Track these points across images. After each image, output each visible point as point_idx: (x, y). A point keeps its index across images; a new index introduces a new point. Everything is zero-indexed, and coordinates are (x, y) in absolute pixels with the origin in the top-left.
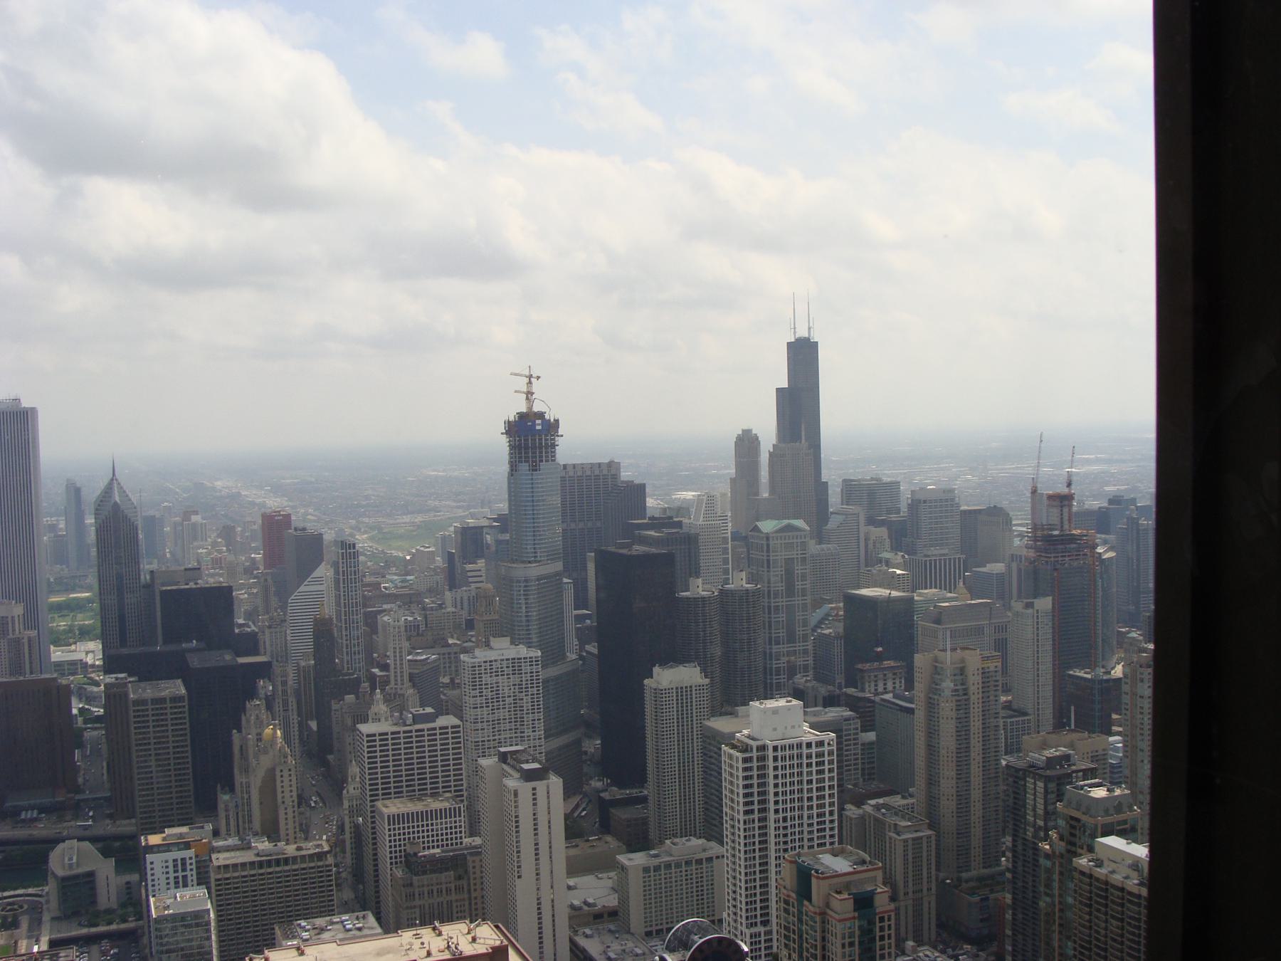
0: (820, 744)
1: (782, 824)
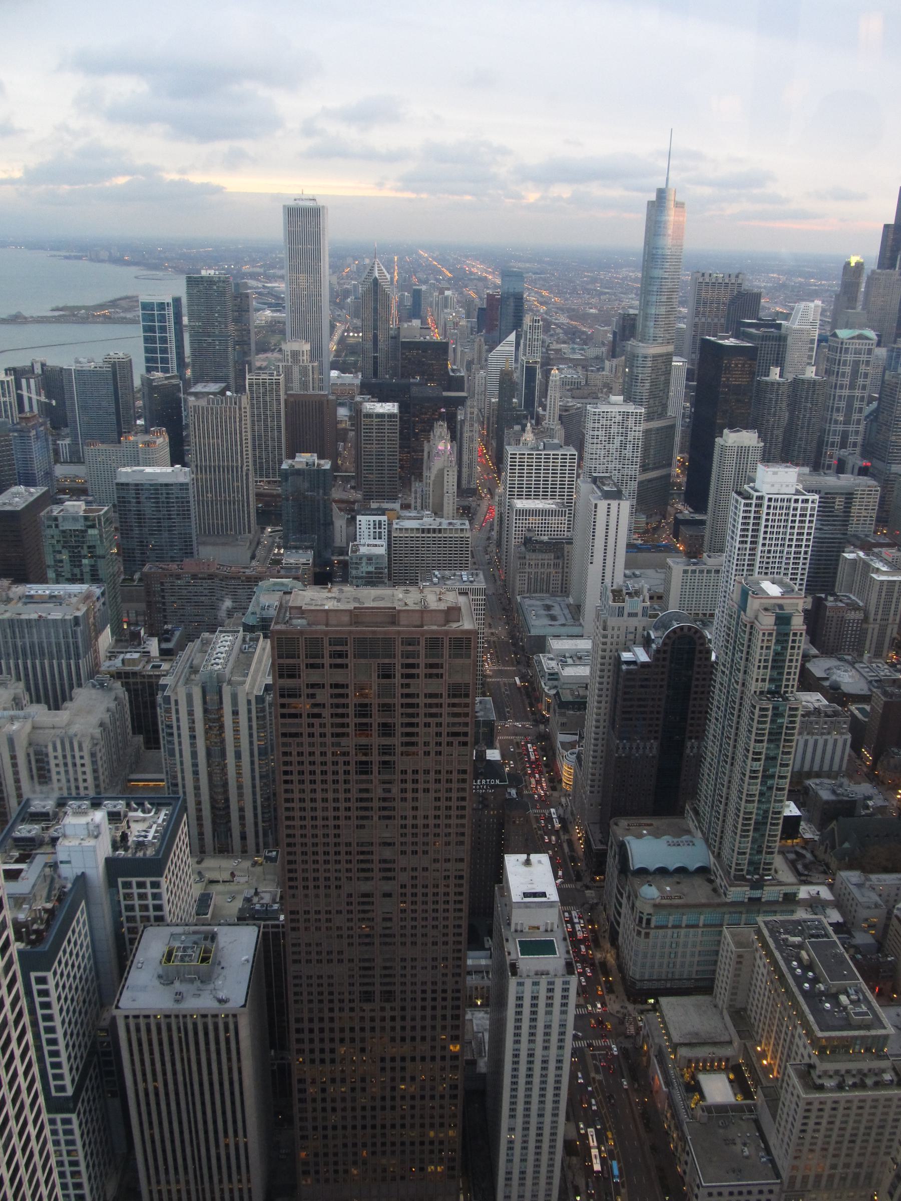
0: (807, 501)
1: (766, 555)
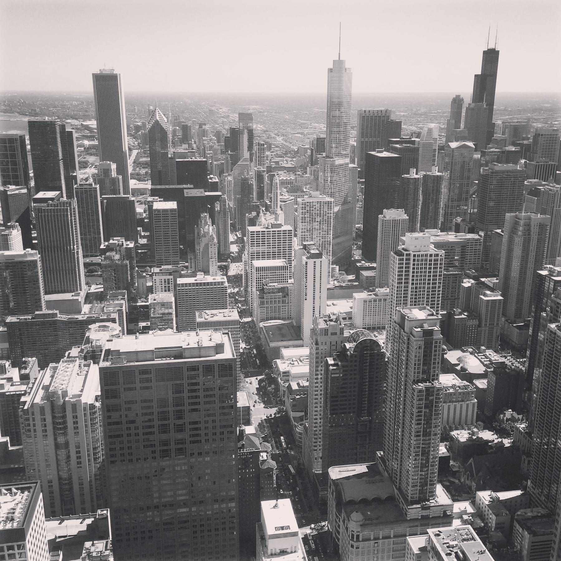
0: (437, 255)
